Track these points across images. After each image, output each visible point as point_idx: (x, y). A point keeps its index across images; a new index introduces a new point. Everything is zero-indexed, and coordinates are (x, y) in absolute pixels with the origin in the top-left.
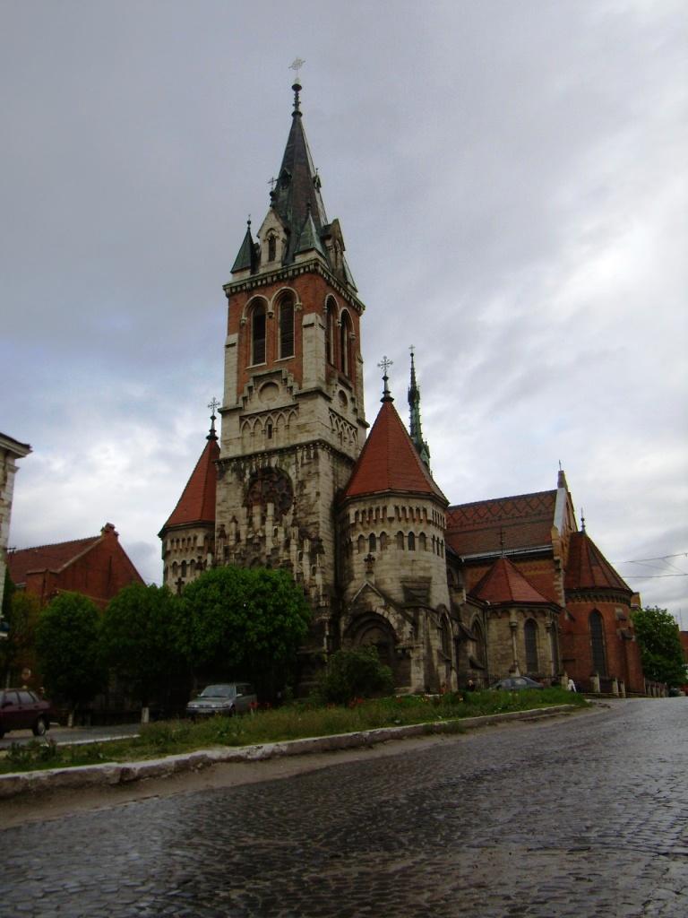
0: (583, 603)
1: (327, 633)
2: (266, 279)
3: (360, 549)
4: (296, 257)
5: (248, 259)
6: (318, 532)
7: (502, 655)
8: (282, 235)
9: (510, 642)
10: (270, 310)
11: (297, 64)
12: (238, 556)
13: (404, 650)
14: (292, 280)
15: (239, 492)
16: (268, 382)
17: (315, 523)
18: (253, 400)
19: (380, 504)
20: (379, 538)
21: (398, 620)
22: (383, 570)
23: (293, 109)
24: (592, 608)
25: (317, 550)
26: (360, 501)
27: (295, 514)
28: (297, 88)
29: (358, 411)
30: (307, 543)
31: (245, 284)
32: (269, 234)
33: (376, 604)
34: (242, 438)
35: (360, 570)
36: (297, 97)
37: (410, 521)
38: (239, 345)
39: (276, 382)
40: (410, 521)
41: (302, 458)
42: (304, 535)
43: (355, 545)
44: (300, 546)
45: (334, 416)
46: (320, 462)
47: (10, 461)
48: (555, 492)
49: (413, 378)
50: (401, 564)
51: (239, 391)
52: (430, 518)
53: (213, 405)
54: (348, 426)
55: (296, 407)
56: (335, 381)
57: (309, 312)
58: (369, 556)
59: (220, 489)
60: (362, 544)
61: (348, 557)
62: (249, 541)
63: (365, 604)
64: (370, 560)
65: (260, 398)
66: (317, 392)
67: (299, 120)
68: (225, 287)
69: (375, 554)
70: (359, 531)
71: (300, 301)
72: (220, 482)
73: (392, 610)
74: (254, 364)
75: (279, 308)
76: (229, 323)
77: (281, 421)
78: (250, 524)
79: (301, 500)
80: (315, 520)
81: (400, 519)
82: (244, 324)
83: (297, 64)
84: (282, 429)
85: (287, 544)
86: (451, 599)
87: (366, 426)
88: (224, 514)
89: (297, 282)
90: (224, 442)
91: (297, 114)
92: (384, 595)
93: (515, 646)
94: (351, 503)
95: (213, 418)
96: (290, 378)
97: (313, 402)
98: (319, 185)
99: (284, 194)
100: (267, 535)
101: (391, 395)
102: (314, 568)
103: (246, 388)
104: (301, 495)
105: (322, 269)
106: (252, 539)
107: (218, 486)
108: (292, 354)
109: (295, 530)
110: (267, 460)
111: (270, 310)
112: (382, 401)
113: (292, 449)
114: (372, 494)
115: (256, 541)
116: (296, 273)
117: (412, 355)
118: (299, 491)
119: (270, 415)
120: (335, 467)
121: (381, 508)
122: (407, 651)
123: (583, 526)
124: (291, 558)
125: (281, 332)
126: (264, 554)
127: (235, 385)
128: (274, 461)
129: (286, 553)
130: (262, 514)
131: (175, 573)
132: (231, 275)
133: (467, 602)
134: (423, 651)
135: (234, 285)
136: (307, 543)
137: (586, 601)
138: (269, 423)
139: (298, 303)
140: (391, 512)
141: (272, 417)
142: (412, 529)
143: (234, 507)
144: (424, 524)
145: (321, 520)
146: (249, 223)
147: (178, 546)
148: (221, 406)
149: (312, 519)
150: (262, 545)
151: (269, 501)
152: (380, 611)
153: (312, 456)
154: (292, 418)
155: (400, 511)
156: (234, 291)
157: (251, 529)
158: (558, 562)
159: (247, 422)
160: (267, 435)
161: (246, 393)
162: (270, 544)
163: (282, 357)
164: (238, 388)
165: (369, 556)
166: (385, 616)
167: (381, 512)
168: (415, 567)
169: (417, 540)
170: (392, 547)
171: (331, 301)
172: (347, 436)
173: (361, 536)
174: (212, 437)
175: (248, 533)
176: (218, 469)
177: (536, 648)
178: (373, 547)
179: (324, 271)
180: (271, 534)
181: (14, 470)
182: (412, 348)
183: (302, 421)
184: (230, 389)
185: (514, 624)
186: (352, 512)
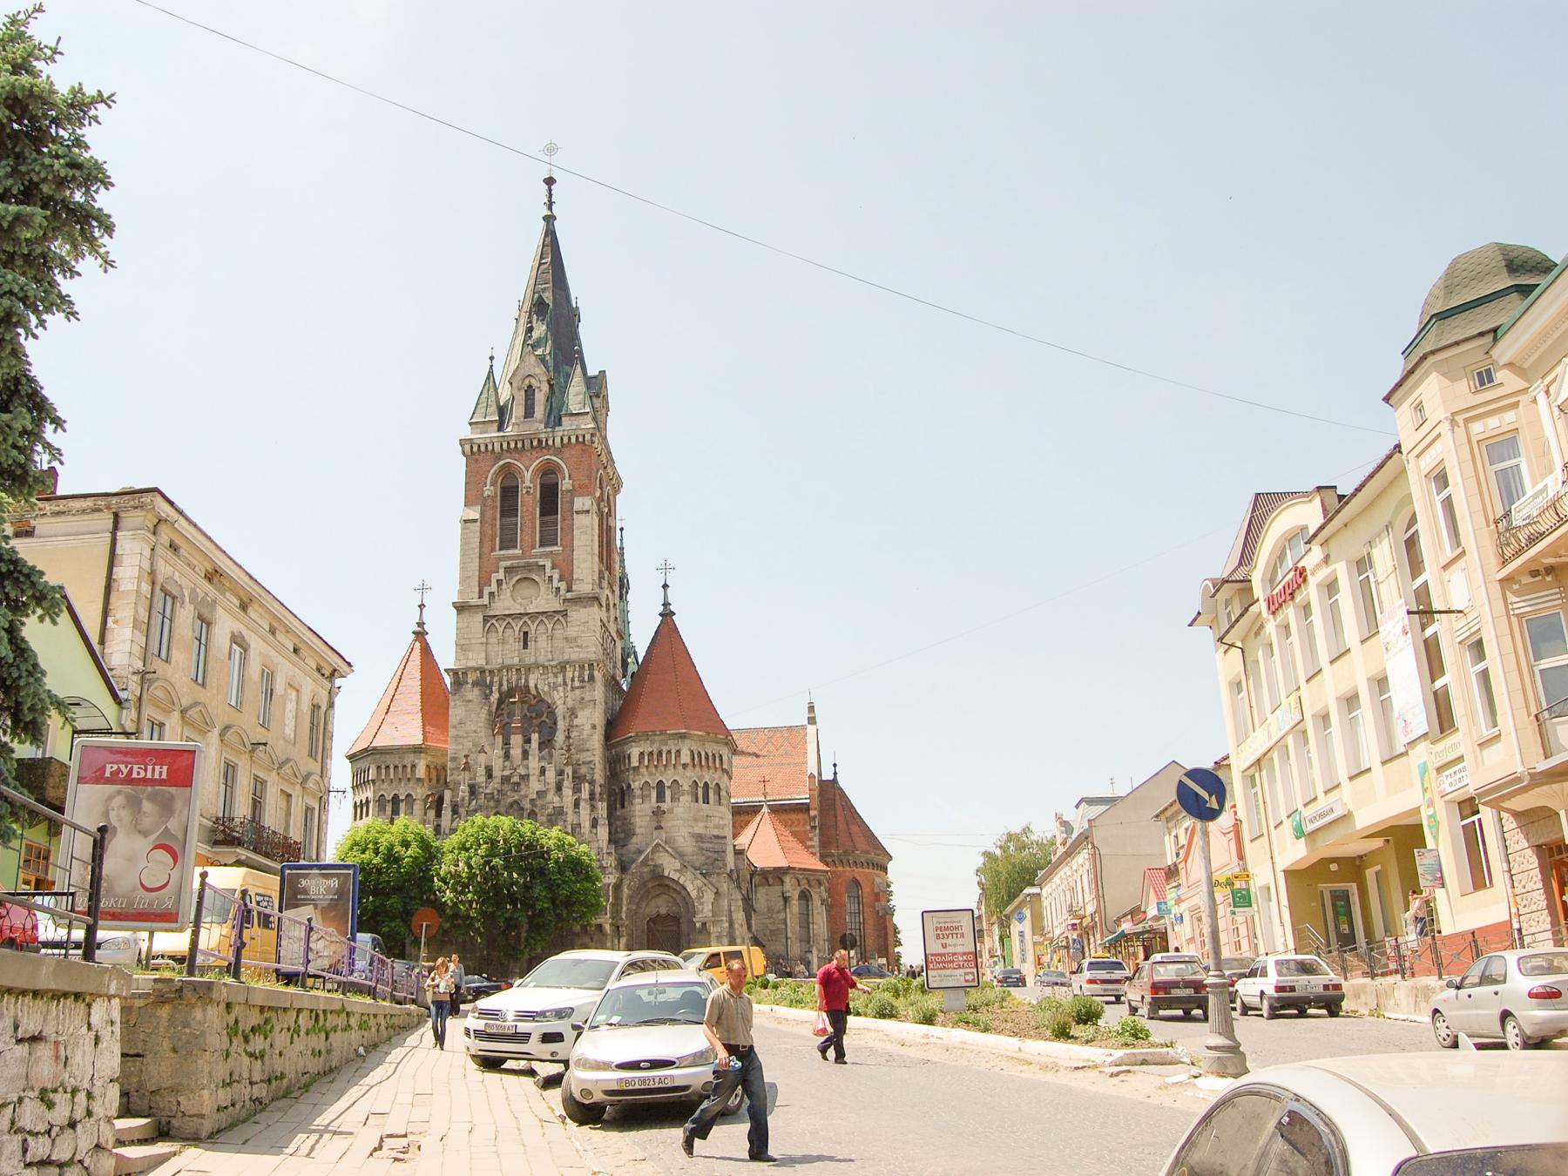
0: (840, 869)
4: (563, 419)
5: (493, 408)
7: (771, 931)
8: (545, 387)
9: (782, 916)
12: (490, 797)
14: (558, 452)
15: (484, 714)
16: (524, 574)
17: (591, 762)
18: (502, 597)
21: (699, 890)
22: (673, 826)
30: (586, 788)
32: (527, 382)
33: (670, 867)
41: (573, 680)
43: (638, 792)
44: (577, 790)
48: (803, 727)
50: (695, 820)
51: (483, 582)
52: (725, 766)
55: (564, 613)
56: (605, 584)
58: (659, 807)
59: (455, 707)
60: (645, 793)
61: (623, 806)
62: (505, 780)
63: (655, 866)
64: (658, 813)
65: (512, 596)
68: (462, 442)
69: (664, 806)
72: (455, 697)
73: (689, 874)
77: (542, 629)
78: (507, 756)
80: (588, 759)
85: (559, 788)
86: (735, 863)
88: (461, 740)
89: (566, 452)
90: (462, 647)
91: (549, 219)
92: (680, 855)
93: (788, 920)
95: (422, 606)
99: (540, 330)
100: (531, 772)
107: (452, 704)
108: (557, 544)
109: (569, 770)
110: (523, 677)
111: (528, 483)
112: (660, 615)
113: (562, 667)
115: (515, 779)
116: (566, 440)
118: (568, 720)
119: (526, 618)
123: (835, 773)
129: (556, 799)
130: (523, 747)
131: (382, 809)
134: (726, 925)
135: (475, 441)
136: (586, 788)
139: (567, 480)
141: (529, 622)
142: (707, 779)
143: (475, 732)
144: (719, 772)
146: (492, 358)
147: (387, 774)
149: (585, 757)
152: (675, 876)
156: (475, 449)
157: (506, 763)
158: (814, 818)
160: (522, 644)
161: (494, 587)
162: (535, 785)
163: (541, 546)
165: (659, 807)
166: (681, 882)
168: (709, 824)
169: (711, 793)
170: (686, 799)
175: (505, 767)
177: (808, 924)
178: (661, 797)
180: (537, 772)
183: (572, 632)
185: (788, 895)
186: (635, 752)
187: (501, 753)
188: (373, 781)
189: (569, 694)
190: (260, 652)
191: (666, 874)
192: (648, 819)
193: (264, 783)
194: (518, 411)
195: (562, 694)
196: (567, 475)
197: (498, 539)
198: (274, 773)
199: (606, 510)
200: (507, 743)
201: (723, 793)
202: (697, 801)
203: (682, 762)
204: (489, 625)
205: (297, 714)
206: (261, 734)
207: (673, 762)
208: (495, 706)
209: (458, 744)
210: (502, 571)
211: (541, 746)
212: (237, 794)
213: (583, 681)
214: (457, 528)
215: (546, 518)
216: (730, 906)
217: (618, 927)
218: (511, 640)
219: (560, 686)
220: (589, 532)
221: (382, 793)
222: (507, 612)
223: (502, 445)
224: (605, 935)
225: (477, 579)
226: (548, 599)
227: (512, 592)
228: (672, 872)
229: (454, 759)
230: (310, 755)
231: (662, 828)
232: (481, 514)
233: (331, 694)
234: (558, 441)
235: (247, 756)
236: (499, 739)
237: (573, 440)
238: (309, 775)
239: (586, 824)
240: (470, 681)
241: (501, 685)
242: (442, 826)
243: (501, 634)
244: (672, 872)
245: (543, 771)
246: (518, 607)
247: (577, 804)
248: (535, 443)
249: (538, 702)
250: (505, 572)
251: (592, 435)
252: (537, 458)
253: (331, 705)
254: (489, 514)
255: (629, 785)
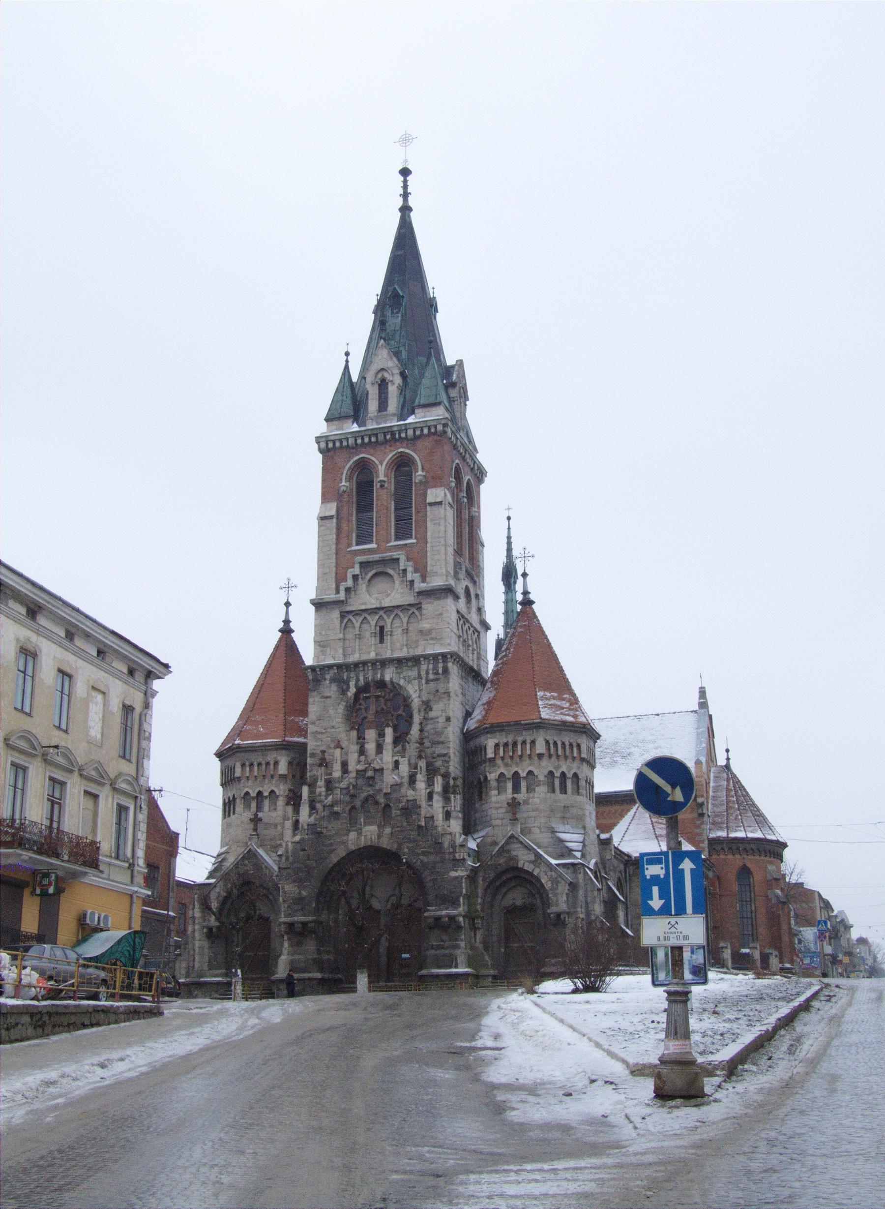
0: (730, 857)
1: (464, 891)
2: (376, 435)
3: (500, 790)
6: (448, 767)
8: (398, 380)
10: (382, 477)
11: (406, 140)
13: (558, 915)
15: (341, 709)
17: (444, 755)
18: (358, 592)
19: (528, 736)
20: (524, 778)
23: (400, 202)
24: (741, 864)
25: (446, 791)
26: (502, 730)
27: (421, 743)
28: (405, 172)
29: (480, 610)
31: (347, 439)
32: (380, 376)
34: (344, 639)
35: (501, 816)
36: (405, 187)
37: (562, 758)
38: (337, 518)
39: (391, 572)
40: (562, 758)
41: (427, 673)
42: (432, 772)
43: (494, 784)
44: (430, 782)
45: (460, 619)
46: (451, 680)
47: (149, 681)
49: (509, 550)
52: (584, 755)
53: (288, 587)
54: (472, 629)
55: (418, 606)
56: (462, 574)
57: (435, 486)
58: (514, 799)
61: (481, 799)
63: (510, 859)
64: (514, 805)
65: (368, 591)
66: (448, 591)
67: (409, 217)
68: (318, 440)
70: (499, 767)
71: (423, 470)
72: (315, 693)
74: (357, 544)
75: (393, 473)
76: (324, 487)
77: (397, 623)
78: (362, 752)
79: (427, 725)
81: (550, 756)
82: (344, 492)
83: (406, 140)
84: (398, 633)
85: (412, 780)
87: (487, 627)
88: (319, 736)
89: (420, 444)
90: (321, 645)
91: (405, 209)
94: (488, 732)
95: (288, 604)
96: (410, 569)
97: (442, 602)
98: (436, 311)
99: (394, 321)
101: (532, 597)
102: (447, 811)
103: (349, 576)
104: (425, 719)
105: (451, 430)
106: (365, 771)
107: (311, 700)
108: (411, 537)
109: (422, 764)
110: (379, 672)
111: (382, 477)
113: (415, 660)
114: (517, 724)
115: (370, 773)
116: (418, 433)
117: (509, 518)
118: (422, 714)
119: (381, 613)
120: (463, 684)
121: (528, 741)
122: (562, 917)
123: (728, 759)
124: (418, 798)
125: (396, 506)
126: (381, 790)
127: (334, 569)
128: (389, 674)
130: (377, 742)
131: (247, 806)
132: (325, 423)
133: (615, 856)
137: (733, 855)
138: (381, 623)
139: (420, 473)
140: (540, 748)
141: (385, 616)
142: (564, 769)
145: (451, 751)
148: (314, 596)
149: (439, 750)
150: (377, 780)
151: (388, 725)
152: (529, 867)
153: (440, 671)
154: (412, 620)
155: (552, 746)
156: (331, 445)
157: (363, 758)
159: (349, 620)
160: (378, 639)
161: (350, 583)
163: (398, 538)
164: (336, 574)
165: (514, 799)
166: (535, 873)
167: (528, 746)
168: (568, 815)
169: (569, 784)
170: (541, 790)
171: (458, 470)
172: (471, 644)
173: (502, 774)
174: (286, 630)
175: (359, 762)
176: (311, 677)
178: (516, 789)
179: (453, 432)
180: (391, 766)
181: (154, 694)
182: (509, 509)
183: (425, 625)
184: (325, 574)
186: (490, 743)
187: (355, 748)
188: (239, 779)
189: (424, 685)
190: (55, 657)
191: (520, 865)
192: (503, 810)
193: (63, 784)
194: (373, 405)
195: (417, 688)
196: (420, 467)
197: (354, 535)
198: (76, 774)
199: (465, 500)
200: (361, 738)
201: (582, 783)
202: (553, 791)
203: (538, 752)
204: (345, 620)
205: (104, 716)
206: (56, 737)
207: (528, 752)
208: (352, 701)
209: (317, 740)
210: (357, 566)
211: (396, 741)
212: (29, 795)
213: (437, 673)
214: (315, 524)
215: (401, 512)
216: (586, 897)
217: (473, 919)
218: (367, 634)
219: (415, 679)
220: (442, 522)
221: (246, 789)
222: (363, 607)
223: (356, 440)
224: (459, 928)
225: (334, 575)
226: (402, 593)
227: (368, 586)
228: (527, 864)
229: (313, 755)
230: (124, 757)
231: (516, 819)
232: (338, 510)
233: (148, 695)
234: (410, 433)
235: (39, 759)
236: (354, 734)
237: (426, 431)
238: (120, 774)
239: (439, 817)
240: (328, 677)
241: (358, 680)
242: (301, 821)
243: (357, 629)
244: (527, 864)
245: (396, 764)
246: (373, 601)
247: (430, 796)
248: (388, 437)
249: (394, 696)
250: (361, 568)
251: (445, 425)
252: (391, 451)
253: (147, 706)
254: (345, 512)
255: (486, 778)
